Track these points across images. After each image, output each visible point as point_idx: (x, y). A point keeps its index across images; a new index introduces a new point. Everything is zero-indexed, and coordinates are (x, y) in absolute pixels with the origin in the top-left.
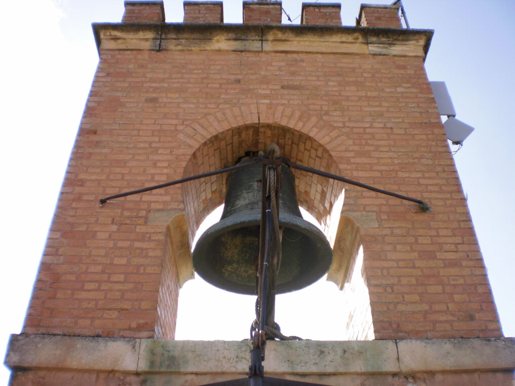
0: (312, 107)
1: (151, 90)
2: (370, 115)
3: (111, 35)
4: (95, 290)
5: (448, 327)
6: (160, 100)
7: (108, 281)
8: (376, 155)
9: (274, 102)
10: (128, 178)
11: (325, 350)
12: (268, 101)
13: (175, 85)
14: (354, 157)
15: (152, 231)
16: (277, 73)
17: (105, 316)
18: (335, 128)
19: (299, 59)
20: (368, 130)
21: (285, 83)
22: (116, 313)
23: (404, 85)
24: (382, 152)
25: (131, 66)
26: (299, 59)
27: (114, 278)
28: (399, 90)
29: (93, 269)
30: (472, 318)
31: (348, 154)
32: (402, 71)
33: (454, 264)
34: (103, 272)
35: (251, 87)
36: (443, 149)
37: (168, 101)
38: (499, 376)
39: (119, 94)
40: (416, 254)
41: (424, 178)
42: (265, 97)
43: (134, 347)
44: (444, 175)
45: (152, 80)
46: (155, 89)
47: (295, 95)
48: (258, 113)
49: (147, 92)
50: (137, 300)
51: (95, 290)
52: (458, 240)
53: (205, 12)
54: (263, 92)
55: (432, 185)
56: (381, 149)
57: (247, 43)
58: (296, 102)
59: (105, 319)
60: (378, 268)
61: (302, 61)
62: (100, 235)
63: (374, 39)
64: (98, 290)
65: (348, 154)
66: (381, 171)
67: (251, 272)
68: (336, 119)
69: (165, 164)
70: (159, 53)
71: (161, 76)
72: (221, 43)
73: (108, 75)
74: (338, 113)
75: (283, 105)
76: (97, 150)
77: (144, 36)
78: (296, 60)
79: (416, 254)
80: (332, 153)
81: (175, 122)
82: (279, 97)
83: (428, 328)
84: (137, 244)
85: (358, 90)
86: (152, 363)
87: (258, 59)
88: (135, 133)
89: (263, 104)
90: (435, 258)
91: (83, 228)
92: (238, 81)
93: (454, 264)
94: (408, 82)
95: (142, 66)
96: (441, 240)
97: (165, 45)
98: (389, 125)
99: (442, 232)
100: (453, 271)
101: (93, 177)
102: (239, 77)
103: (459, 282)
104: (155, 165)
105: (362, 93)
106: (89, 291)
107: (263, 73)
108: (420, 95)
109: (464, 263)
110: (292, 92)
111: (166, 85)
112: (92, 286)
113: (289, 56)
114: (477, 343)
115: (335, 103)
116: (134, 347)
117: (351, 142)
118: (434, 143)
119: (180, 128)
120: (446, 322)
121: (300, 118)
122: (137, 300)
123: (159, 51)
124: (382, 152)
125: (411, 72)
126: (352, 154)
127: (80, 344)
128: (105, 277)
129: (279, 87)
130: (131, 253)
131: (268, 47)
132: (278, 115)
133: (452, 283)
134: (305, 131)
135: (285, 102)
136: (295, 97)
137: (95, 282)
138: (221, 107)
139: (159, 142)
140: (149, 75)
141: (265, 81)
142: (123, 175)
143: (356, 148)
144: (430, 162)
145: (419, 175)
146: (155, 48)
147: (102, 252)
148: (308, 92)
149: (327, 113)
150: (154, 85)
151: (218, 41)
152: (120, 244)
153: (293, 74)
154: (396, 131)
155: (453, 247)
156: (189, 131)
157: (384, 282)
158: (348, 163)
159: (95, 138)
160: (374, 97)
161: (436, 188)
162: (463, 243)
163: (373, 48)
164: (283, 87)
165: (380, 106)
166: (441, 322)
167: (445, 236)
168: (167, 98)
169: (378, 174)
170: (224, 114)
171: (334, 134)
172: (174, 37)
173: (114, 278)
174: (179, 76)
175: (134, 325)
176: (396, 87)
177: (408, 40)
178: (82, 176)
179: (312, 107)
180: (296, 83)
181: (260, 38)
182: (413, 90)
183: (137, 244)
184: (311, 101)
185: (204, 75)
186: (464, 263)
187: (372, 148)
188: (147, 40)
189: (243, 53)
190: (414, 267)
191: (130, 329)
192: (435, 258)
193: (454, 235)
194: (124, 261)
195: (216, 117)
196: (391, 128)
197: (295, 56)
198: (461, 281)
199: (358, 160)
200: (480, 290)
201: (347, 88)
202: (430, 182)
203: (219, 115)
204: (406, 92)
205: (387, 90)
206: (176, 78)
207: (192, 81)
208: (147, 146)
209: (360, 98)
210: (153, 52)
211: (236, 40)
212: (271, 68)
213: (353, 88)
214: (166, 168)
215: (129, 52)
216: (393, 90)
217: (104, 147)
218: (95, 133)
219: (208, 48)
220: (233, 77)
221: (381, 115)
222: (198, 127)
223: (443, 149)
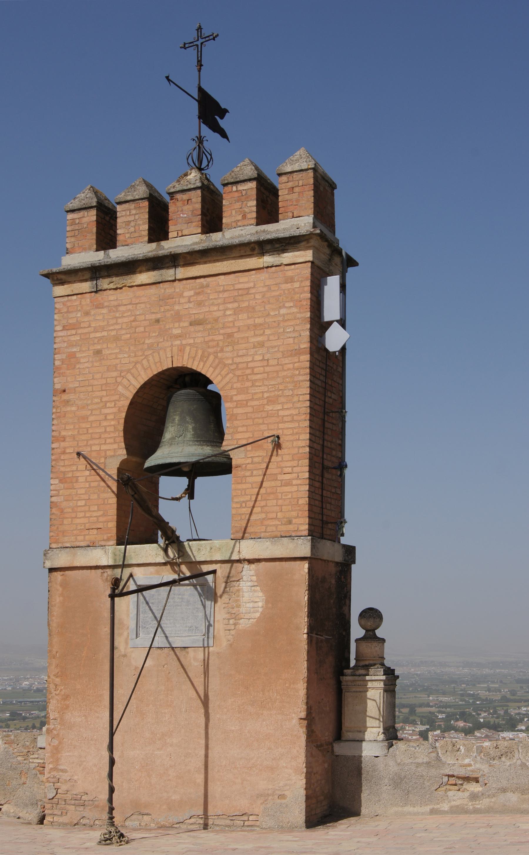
1: (96, 341)
2: (254, 347)
3: (57, 279)
4: (83, 517)
5: (274, 529)
6: (104, 352)
7: (89, 511)
8: (252, 390)
10: (90, 431)
11: (201, 548)
14: (236, 395)
16: (187, 307)
17: (91, 533)
18: (225, 365)
19: (205, 283)
22: (96, 530)
23: (287, 305)
24: (257, 386)
26: (205, 283)
27: (92, 509)
28: (283, 311)
29: (80, 503)
30: (290, 522)
32: (289, 286)
33: (288, 483)
34: (85, 505)
39: (74, 350)
41: (283, 409)
42: (177, 337)
43: (105, 552)
44: (298, 405)
45: (96, 331)
47: (199, 331)
48: (172, 357)
50: (105, 522)
51: (83, 517)
52: (295, 463)
53: (134, 212)
55: (287, 416)
57: (163, 271)
59: (91, 535)
60: (239, 489)
61: (208, 286)
62: (81, 479)
63: (268, 247)
64: (85, 517)
65: (234, 392)
66: (253, 407)
69: (112, 417)
70: (97, 295)
75: (190, 345)
76: (69, 409)
77: (83, 276)
78: (202, 287)
81: (115, 374)
82: (188, 336)
83: (262, 530)
85: (249, 318)
86: (115, 560)
88: (90, 389)
89: (175, 346)
91: (70, 475)
92: (158, 321)
93: (288, 483)
95: (87, 314)
97: (101, 285)
102: (159, 316)
103: (288, 497)
104: (106, 419)
105: (250, 322)
106: (80, 518)
108: (299, 316)
109: (294, 482)
111: (105, 334)
112: (82, 515)
113: (198, 281)
114: (285, 540)
116: (105, 552)
118: (297, 372)
120: (274, 525)
121: (201, 360)
122: (105, 522)
123: (96, 292)
124: (257, 386)
127: (79, 551)
128: (87, 508)
130: (99, 491)
132: (186, 357)
133: (283, 497)
135: (191, 341)
136: (199, 335)
137: (82, 512)
138: (146, 353)
139: (107, 395)
141: (178, 317)
144: (291, 393)
145: (279, 407)
146: (93, 290)
148: (209, 326)
149: (222, 351)
150: (98, 335)
153: (200, 304)
154: (271, 362)
155: (290, 470)
156: (125, 382)
157: (242, 499)
158: (231, 400)
159: (65, 397)
160: (261, 325)
161: (289, 419)
162: (298, 466)
164: (191, 324)
165: (263, 334)
166: (271, 526)
167: (286, 461)
172: (106, 274)
173: (92, 509)
175: (105, 538)
176: (280, 308)
180: (201, 317)
181: (173, 264)
182: (294, 310)
184: (211, 337)
189: (161, 284)
191: (104, 540)
193: (293, 460)
195: (142, 365)
196: (268, 360)
197: (202, 280)
203: (145, 362)
204: (288, 314)
208: (99, 401)
209: (248, 327)
210: (93, 294)
213: (245, 316)
215: (74, 297)
216: (277, 313)
217: (72, 405)
220: (154, 317)
221: (261, 345)
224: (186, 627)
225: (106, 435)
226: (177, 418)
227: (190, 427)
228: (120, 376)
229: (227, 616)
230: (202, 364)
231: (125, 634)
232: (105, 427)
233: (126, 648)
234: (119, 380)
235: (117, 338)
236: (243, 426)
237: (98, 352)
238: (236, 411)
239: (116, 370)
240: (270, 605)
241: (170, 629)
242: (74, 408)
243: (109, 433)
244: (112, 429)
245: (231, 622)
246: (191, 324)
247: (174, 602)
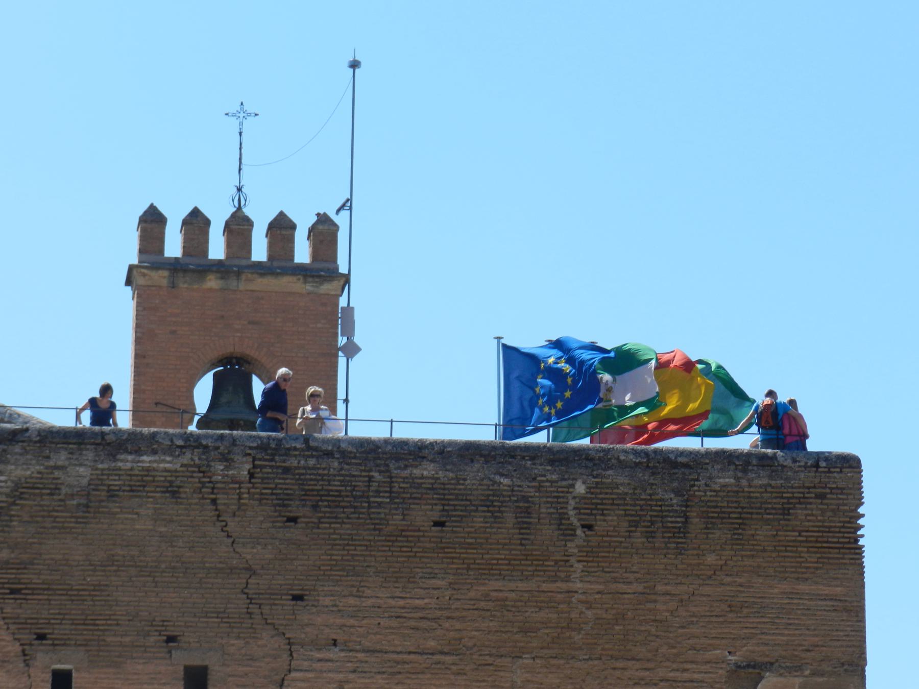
12: (239, 334)
28: (319, 325)
63: (310, 279)
72: (212, 282)
73: (145, 309)
92: (222, 317)
119: (191, 355)
123: (173, 287)
129: (246, 323)
131: (242, 286)
150: (174, 319)
151: (210, 280)
163: (309, 287)
164: (249, 323)
178: (143, 387)
188: (164, 277)
211: (222, 278)
215: (153, 288)
218: (144, 357)
226: (231, 388)
227: (242, 396)
246: (249, 323)
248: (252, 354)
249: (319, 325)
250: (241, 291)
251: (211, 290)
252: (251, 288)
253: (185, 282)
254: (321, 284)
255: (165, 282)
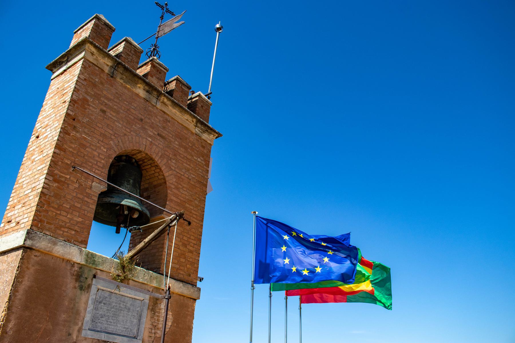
0: (166, 152)
2: (185, 169)
8: (181, 190)
9: (153, 141)
12: (150, 140)
13: (115, 107)
15: (93, 194)
18: (172, 169)
20: (182, 177)
21: (160, 132)
25: (97, 80)
28: (199, 160)
30: (190, 276)
31: (173, 186)
32: (202, 149)
33: (191, 252)
35: (146, 127)
36: (203, 199)
37: (110, 116)
38: (192, 300)
40: (181, 243)
46: (106, 104)
49: (102, 104)
54: (150, 133)
56: (184, 189)
58: (161, 147)
63: (199, 125)
67: (100, 211)
68: (173, 164)
71: (109, 96)
74: (174, 161)
75: (156, 145)
79: (181, 243)
80: (167, 183)
81: (111, 132)
84: (86, 199)
87: (153, 110)
90: (186, 247)
93: (191, 252)
94: (203, 157)
95: (102, 83)
96: (191, 240)
98: (190, 178)
99: (192, 237)
100: (190, 254)
101: (71, 150)
102: (143, 118)
105: (185, 155)
107: (153, 121)
108: (205, 167)
110: (161, 139)
111: (111, 104)
114: (190, 286)
115: (175, 155)
117: (175, 180)
119: (113, 137)
120: (182, 274)
121: (161, 157)
123: (112, 77)
125: (205, 151)
126: (173, 186)
129: (156, 133)
134: (161, 165)
135: (157, 144)
136: (161, 143)
140: (105, 93)
141: (152, 126)
142: (84, 155)
143: (176, 184)
144: (197, 203)
147: (70, 197)
149: (170, 160)
152: (79, 196)
163: (197, 130)
164: (158, 134)
168: (111, 114)
169: (179, 201)
170: (132, 138)
171: (170, 172)
174: (118, 101)
177: (211, 133)
178: (65, 146)
179: (166, 152)
180: (164, 135)
183: (86, 199)
185: (129, 108)
186: (194, 253)
187: (181, 186)
188: (108, 65)
190: (179, 249)
192: (186, 247)
194: (79, 206)
195: (128, 138)
197: (167, 117)
198: (191, 260)
199: (175, 191)
200: (196, 266)
201: (181, 149)
202: (194, 213)
205: (195, 158)
206: (116, 102)
207: (123, 108)
211: (147, 92)
212: (157, 119)
213: (183, 150)
214: (103, 159)
215: (97, 68)
217: (77, 132)
218: (74, 120)
219: (134, 90)
220: (140, 116)
222: (120, 141)
223: (203, 199)
224: (124, 328)
225: (96, 167)
226: (131, 181)
228: (114, 136)
229: (151, 326)
230: (160, 161)
231: (80, 324)
232: (97, 161)
233: (77, 337)
234: (113, 137)
235: (118, 112)
236: (174, 208)
237: (104, 112)
238: (173, 198)
239: (112, 130)
240: (175, 325)
241: (113, 327)
242: (78, 134)
243: (99, 167)
244: (101, 166)
245: (153, 331)
246: (158, 134)
247: (120, 307)
248: (156, 160)
249: (199, 160)
250: (157, 108)
251: (137, 95)
252: (163, 109)
253: (121, 79)
254: (204, 132)
255: (107, 70)
